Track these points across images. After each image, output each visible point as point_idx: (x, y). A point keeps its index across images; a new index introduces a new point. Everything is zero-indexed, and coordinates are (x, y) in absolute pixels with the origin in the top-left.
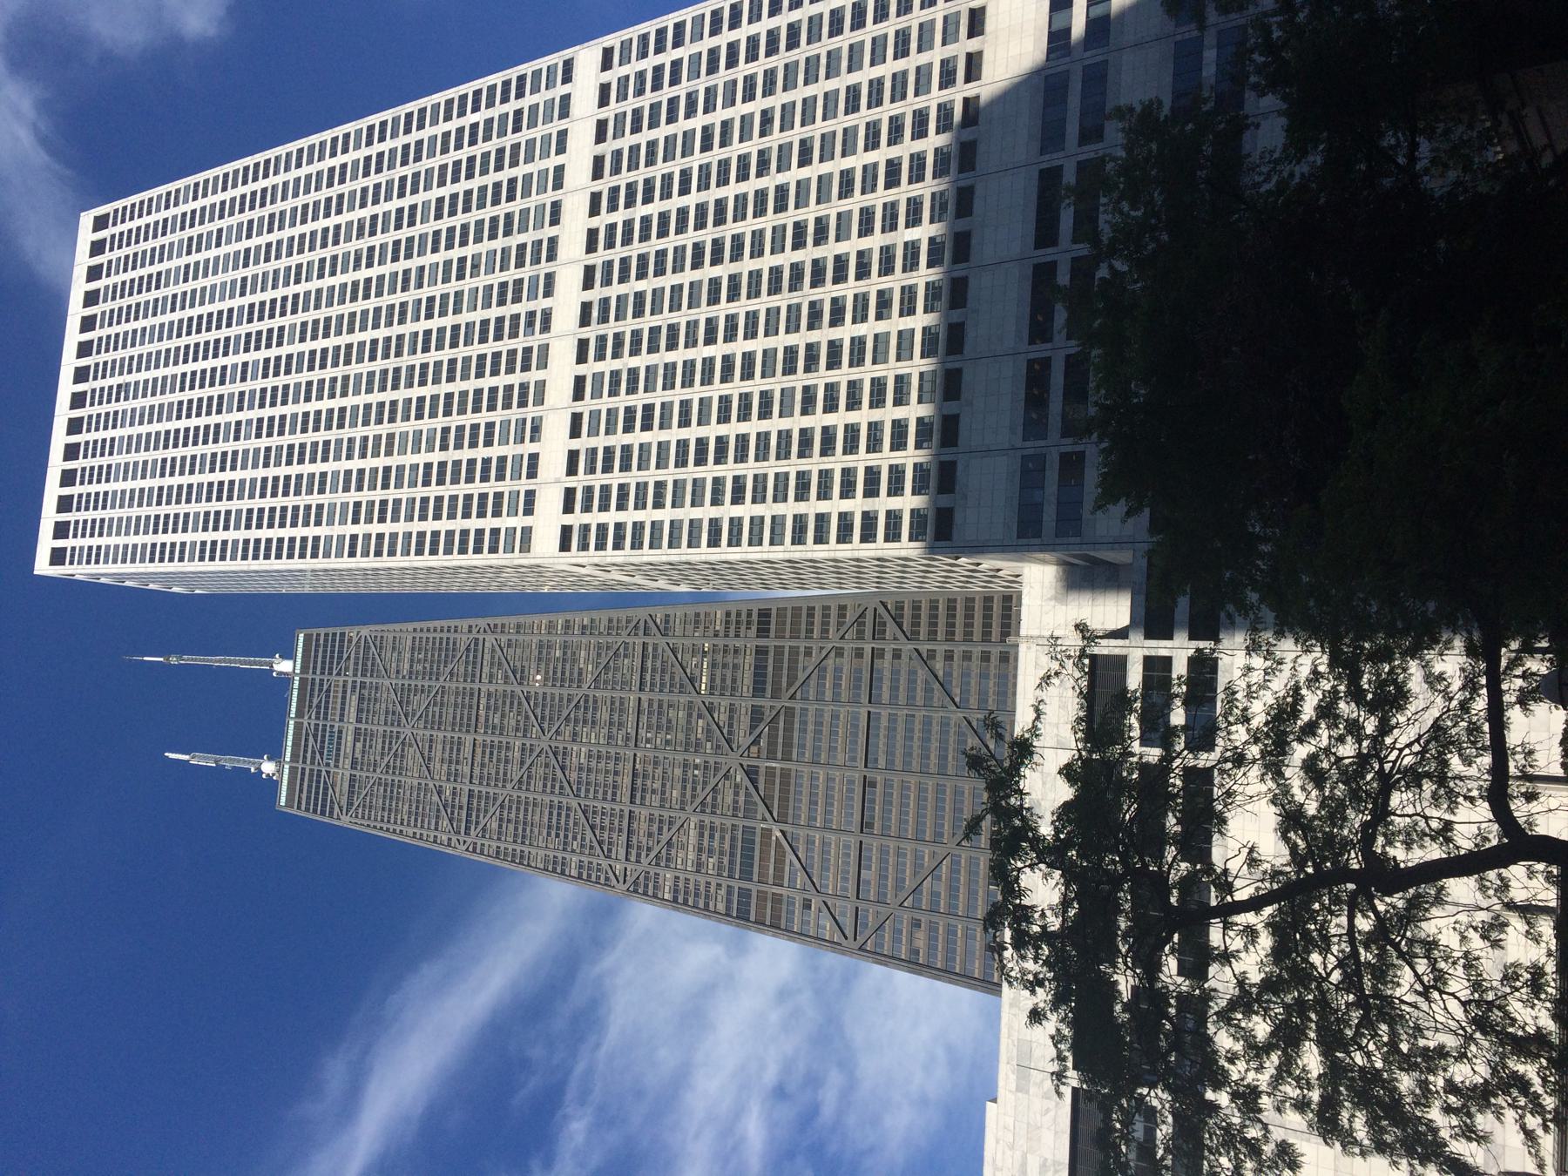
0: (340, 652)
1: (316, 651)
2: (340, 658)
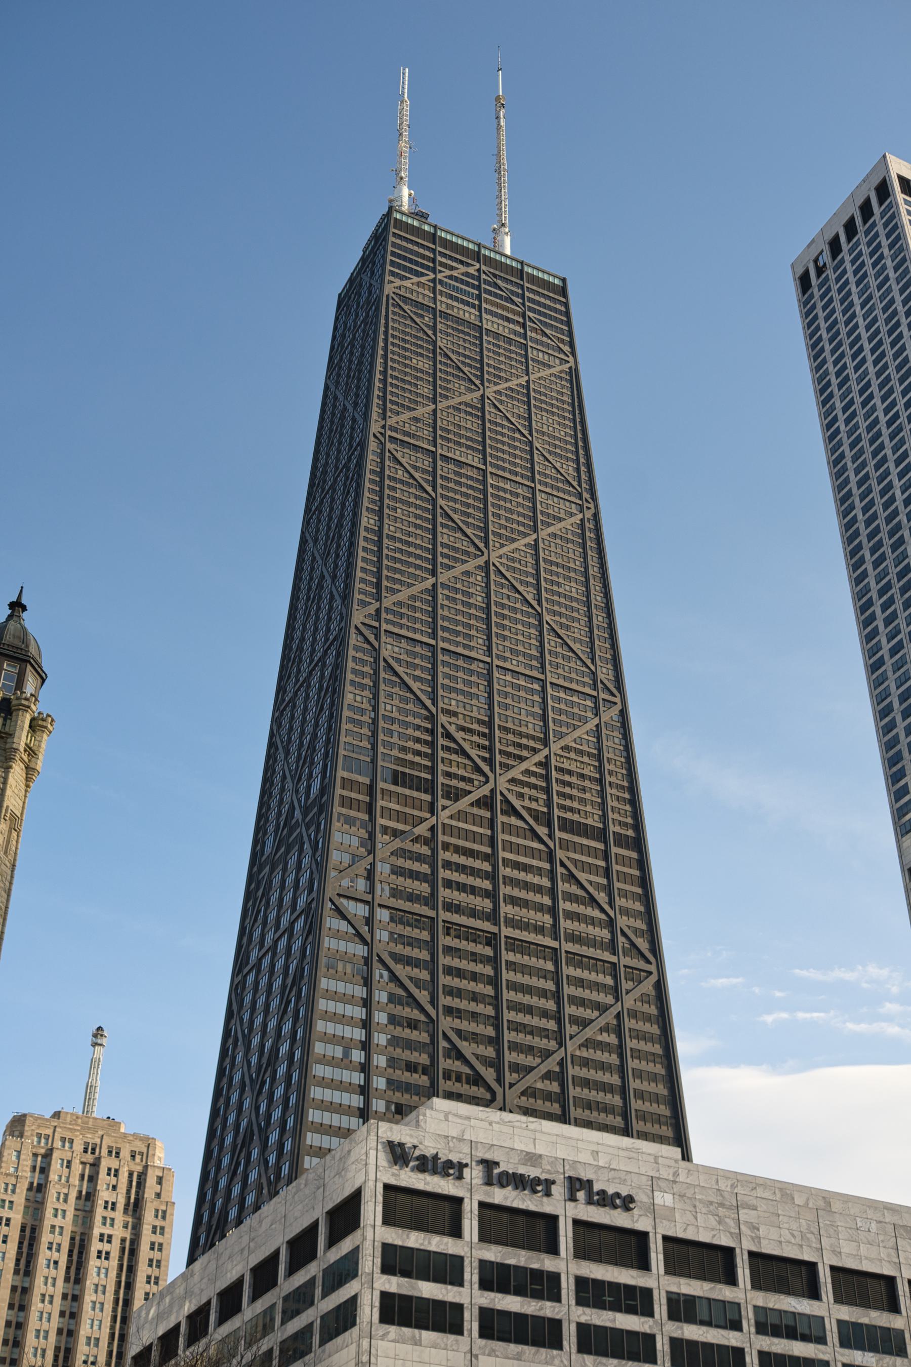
2: (546, 324)
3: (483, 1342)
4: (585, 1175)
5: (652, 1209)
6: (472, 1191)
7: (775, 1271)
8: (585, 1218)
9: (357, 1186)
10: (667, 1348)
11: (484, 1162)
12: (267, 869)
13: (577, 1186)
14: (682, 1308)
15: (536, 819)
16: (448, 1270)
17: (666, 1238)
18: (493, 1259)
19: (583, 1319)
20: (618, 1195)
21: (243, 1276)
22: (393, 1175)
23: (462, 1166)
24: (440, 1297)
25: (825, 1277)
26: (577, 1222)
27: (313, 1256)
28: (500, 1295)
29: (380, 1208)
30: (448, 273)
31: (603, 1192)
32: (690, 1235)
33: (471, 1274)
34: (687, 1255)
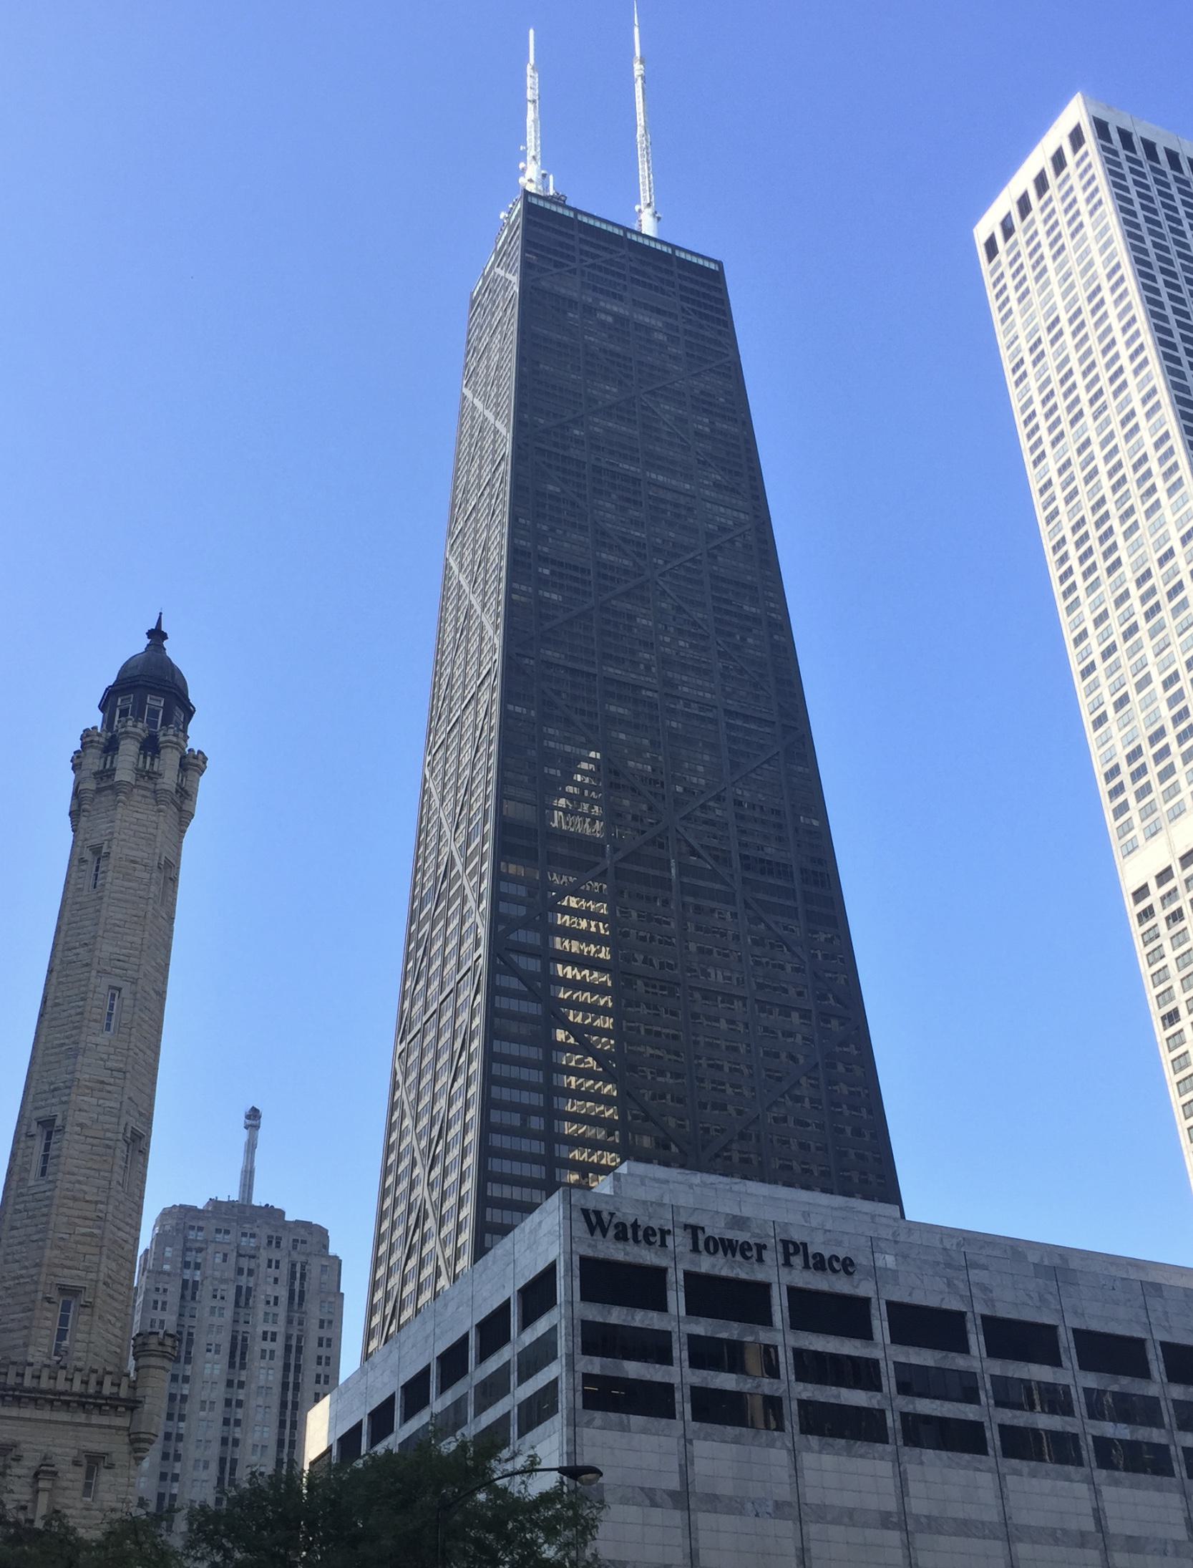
0: (707, 317)
1: (703, 285)
3: (697, 1425)
4: (797, 1237)
5: (875, 1273)
6: (678, 1262)
7: (1014, 1339)
8: (801, 1285)
9: (551, 1259)
10: (898, 1425)
11: (686, 1227)
12: (427, 927)
13: (791, 1249)
14: (910, 1382)
15: (716, 858)
16: (655, 1347)
17: (890, 1304)
18: (703, 1334)
19: (805, 1396)
20: (837, 1259)
21: (429, 1365)
22: (589, 1246)
23: (664, 1233)
24: (648, 1377)
25: (1066, 1340)
26: (792, 1291)
27: (505, 1339)
28: (712, 1373)
29: (577, 1283)
30: (590, 261)
31: (818, 1256)
32: (919, 1299)
33: (680, 1352)
34: (914, 1323)
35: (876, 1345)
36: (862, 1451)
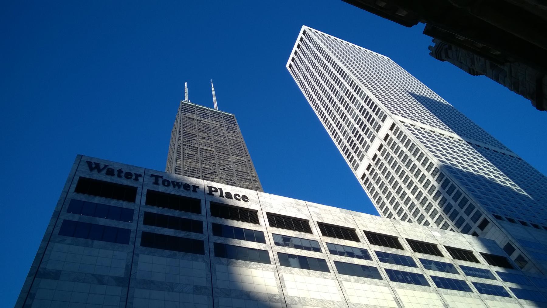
11: (152, 175)
18: (156, 212)
19: (219, 242)
35: (262, 226)
36: (255, 266)
